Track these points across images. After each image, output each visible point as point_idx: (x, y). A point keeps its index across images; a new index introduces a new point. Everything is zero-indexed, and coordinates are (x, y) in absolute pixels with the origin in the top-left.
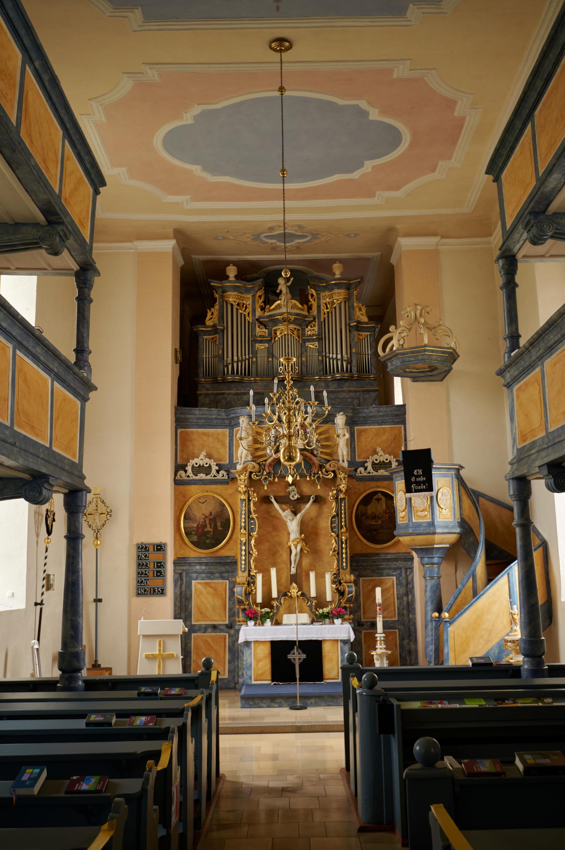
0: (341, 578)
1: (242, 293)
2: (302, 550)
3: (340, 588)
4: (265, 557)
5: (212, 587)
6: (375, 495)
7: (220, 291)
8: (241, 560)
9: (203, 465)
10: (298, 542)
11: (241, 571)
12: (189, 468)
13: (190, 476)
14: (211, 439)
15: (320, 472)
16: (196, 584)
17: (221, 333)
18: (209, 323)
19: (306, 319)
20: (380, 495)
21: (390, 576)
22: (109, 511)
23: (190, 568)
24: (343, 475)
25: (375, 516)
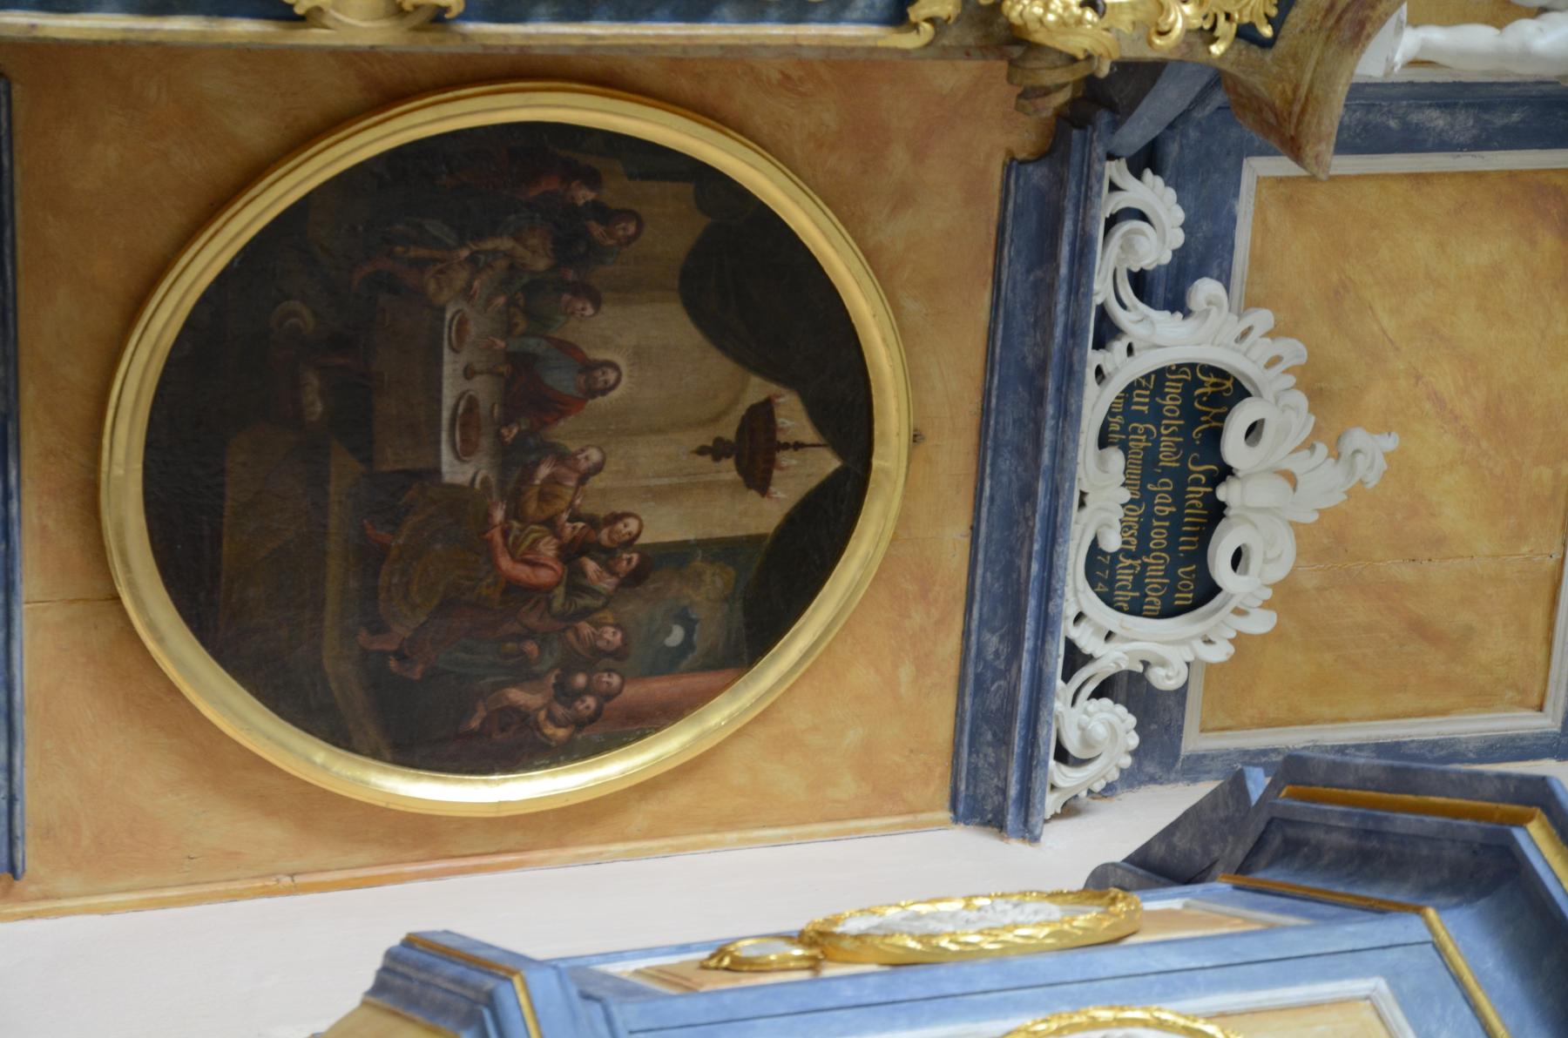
6: (819, 413)
25: (555, 406)
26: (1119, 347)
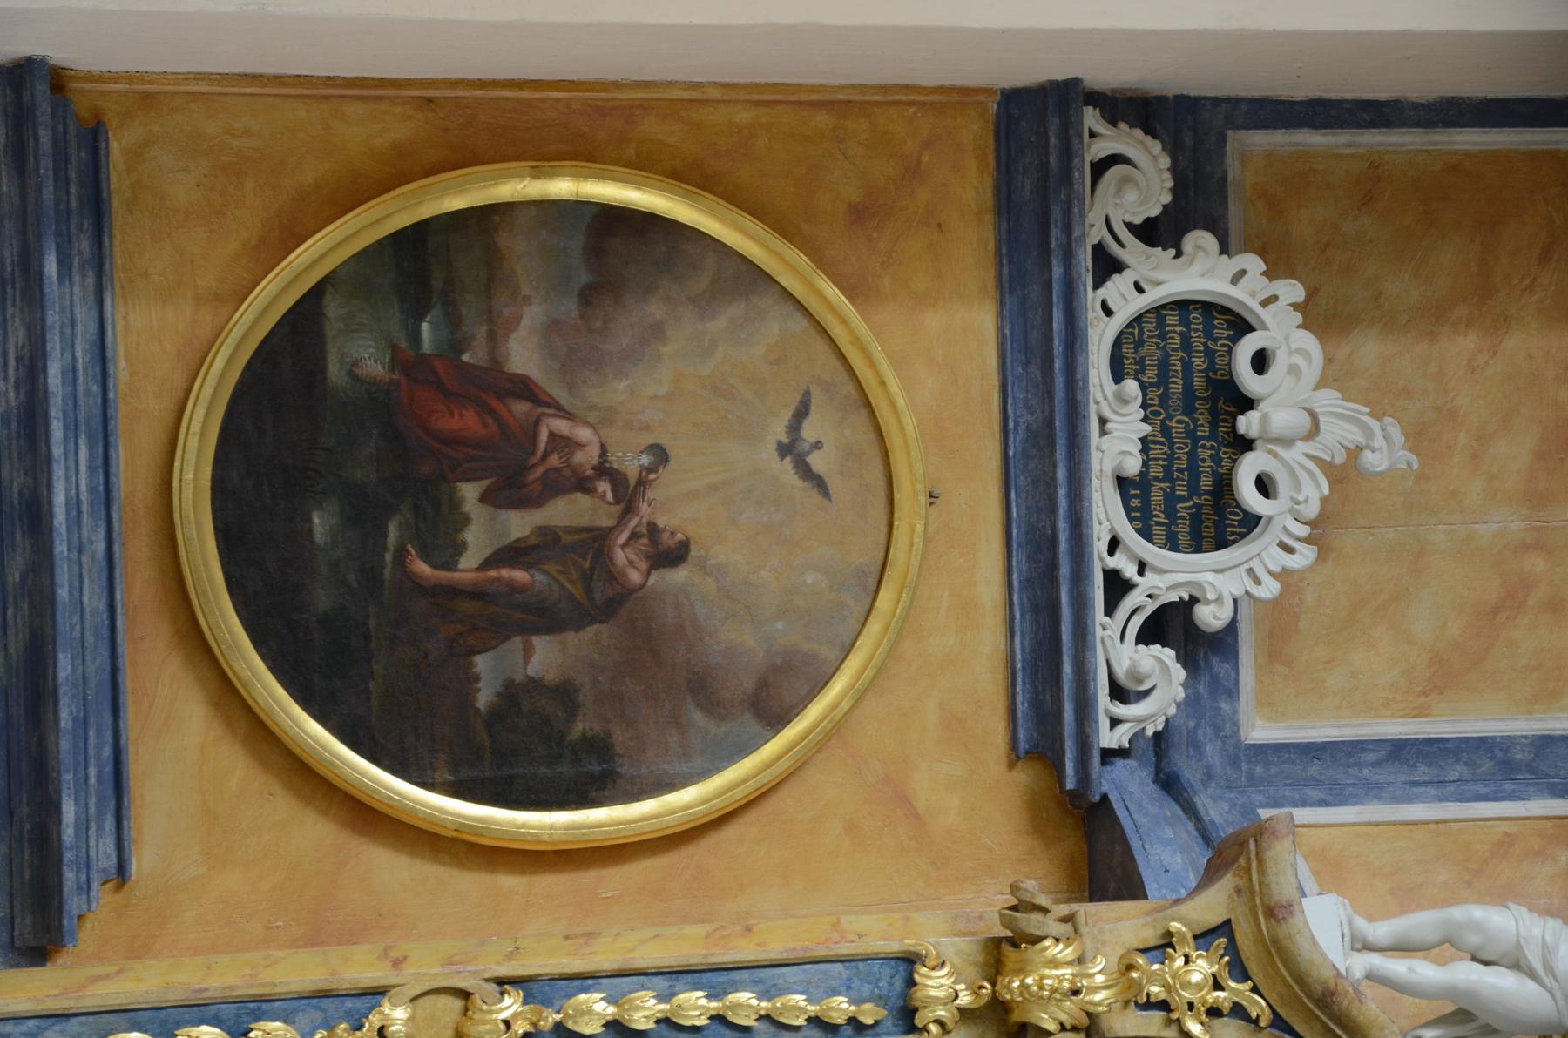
13: (1117, 289)
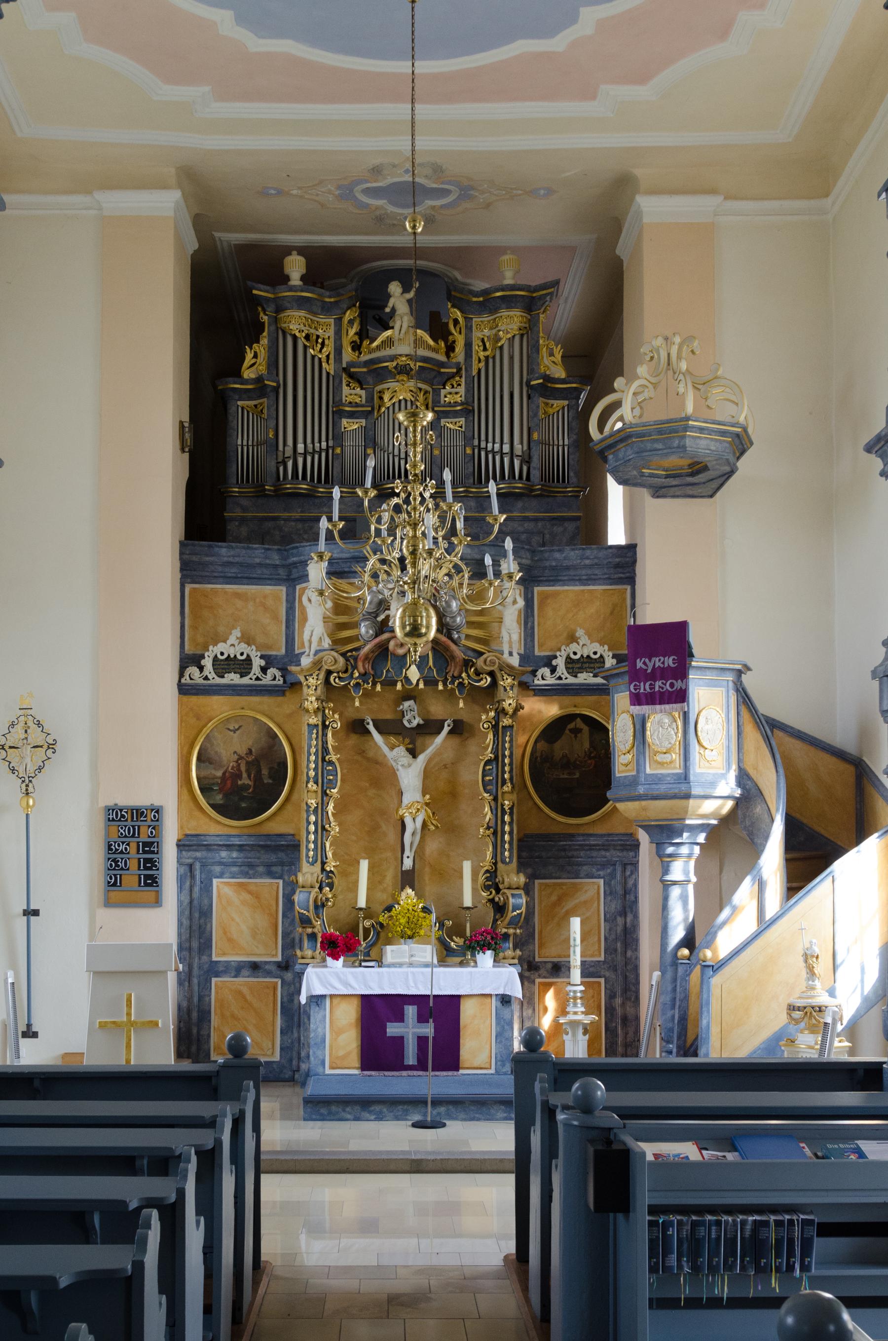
0: (501, 879)
1: (315, 314)
2: (424, 825)
3: (497, 899)
4: (354, 838)
5: (250, 893)
7: (270, 309)
8: (308, 842)
9: (235, 656)
10: (418, 810)
11: (308, 862)
12: (207, 663)
13: (210, 677)
14: (251, 606)
15: (464, 675)
16: (221, 886)
17: (272, 396)
18: (248, 374)
19: (442, 370)
20: (579, 723)
21: (592, 877)
22: (51, 742)
23: (210, 855)
24: (509, 680)
26: (562, 676)
